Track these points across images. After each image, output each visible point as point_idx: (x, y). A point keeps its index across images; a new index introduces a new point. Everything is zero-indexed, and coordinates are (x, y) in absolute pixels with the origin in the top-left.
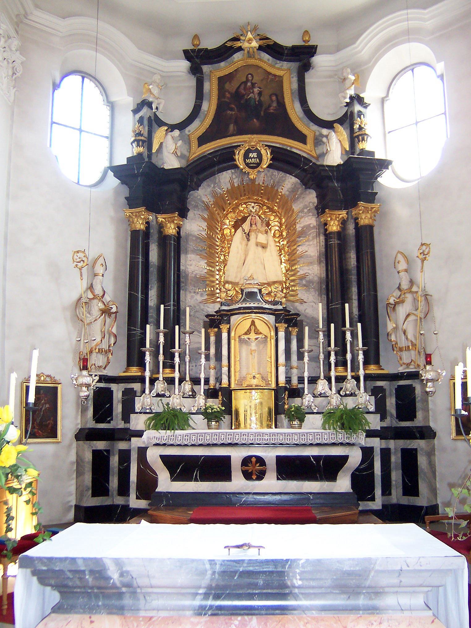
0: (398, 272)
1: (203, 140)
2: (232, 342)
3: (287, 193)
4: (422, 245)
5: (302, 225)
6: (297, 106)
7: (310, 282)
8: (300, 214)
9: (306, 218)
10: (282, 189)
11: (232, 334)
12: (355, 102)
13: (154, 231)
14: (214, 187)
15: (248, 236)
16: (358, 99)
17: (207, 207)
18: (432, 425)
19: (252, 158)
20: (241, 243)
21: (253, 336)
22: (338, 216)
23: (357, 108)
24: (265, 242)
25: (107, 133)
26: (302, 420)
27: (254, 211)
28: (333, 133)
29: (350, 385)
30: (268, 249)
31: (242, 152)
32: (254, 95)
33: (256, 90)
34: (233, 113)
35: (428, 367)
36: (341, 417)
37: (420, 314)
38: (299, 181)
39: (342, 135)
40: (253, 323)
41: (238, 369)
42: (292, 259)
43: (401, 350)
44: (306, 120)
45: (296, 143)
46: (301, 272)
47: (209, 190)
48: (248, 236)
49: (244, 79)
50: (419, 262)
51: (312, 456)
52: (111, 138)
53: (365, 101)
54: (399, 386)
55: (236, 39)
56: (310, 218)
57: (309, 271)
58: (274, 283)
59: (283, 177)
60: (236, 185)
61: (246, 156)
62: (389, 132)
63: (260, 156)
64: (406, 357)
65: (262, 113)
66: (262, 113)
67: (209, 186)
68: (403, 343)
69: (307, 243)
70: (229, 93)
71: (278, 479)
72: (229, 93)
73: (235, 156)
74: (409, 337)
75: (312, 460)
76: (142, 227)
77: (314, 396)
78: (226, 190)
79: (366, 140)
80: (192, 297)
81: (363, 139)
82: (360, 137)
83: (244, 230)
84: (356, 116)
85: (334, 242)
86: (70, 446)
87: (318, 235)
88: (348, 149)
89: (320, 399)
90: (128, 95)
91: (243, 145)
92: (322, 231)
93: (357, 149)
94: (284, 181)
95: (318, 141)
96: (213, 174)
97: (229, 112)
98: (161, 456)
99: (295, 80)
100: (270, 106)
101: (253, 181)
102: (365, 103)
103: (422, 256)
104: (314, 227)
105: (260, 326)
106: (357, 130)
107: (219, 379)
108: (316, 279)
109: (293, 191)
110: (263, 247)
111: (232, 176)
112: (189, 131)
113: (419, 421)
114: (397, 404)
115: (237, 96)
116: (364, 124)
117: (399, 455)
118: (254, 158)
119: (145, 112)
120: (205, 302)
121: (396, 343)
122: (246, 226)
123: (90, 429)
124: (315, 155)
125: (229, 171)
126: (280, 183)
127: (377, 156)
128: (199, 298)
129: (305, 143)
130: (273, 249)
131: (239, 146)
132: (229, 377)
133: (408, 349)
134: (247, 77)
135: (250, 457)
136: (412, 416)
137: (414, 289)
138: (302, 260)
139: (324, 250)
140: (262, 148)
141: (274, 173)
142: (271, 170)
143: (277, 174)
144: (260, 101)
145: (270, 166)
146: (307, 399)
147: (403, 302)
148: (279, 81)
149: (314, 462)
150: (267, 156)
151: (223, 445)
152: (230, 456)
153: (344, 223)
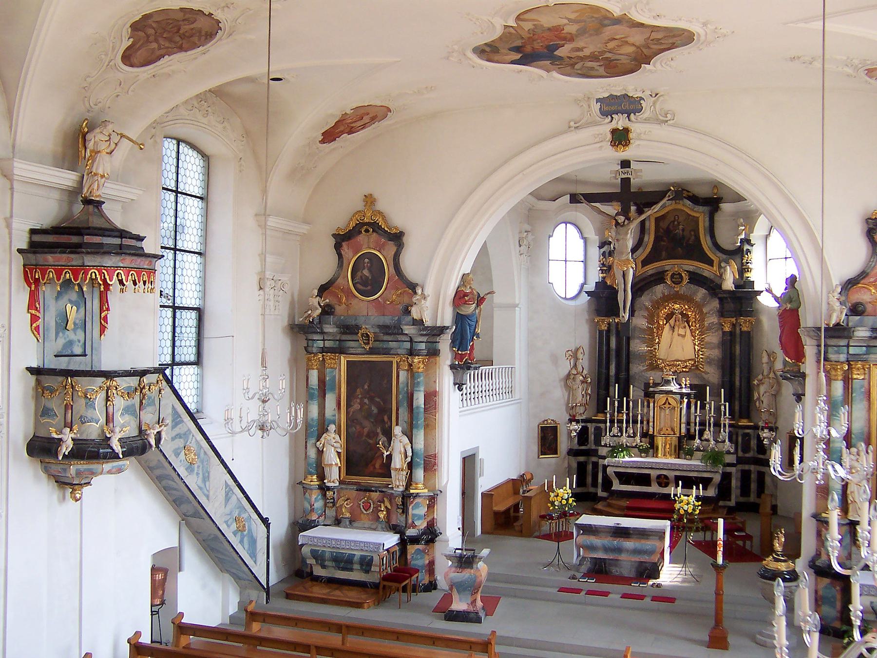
1: (645, 263)
2: (656, 409)
5: (709, 322)
6: (708, 238)
7: (713, 360)
11: (656, 405)
12: (745, 243)
13: (613, 329)
14: (652, 295)
16: (748, 241)
17: (647, 308)
19: (676, 278)
23: (746, 247)
25: (582, 258)
26: (692, 456)
32: (679, 231)
33: (681, 227)
41: (658, 424)
44: (714, 249)
46: (707, 354)
47: (649, 296)
48: (673, 328)
49: (673, 219)
52: (585, 262)
58: (690, 360)
60: (666, 294)
63: (681, 277)
67: (648, 294)
70: (663, 229)
72: (663, 229)
76: (606, 328)
77: (701, 440)
84: (745, 253)
86: (565, 458)
90: (596, 235)
98: (614, 472)
99: (707, 219)
100: (689, 239)
101: (678, 291)
105: (671, 400)
107: (648, 430)
108: (716, 358)
109: (704, 299)
115: (668, 231)
117: (756, 473)
119: (605, 248)
120: (647, 370)
122: (672, 321)
123: (576, 450)
125: (662, 285)
126: (695, 293)
128: (641, 368)
129: (713, 266)
130: (688, 336)
132: (654, 428)
134: (675, 218)
144: (683, 235)
146: (697, 441)
147: (763, 383)
148: (696, 221)
152: (650, 474)
153: (734, 325)
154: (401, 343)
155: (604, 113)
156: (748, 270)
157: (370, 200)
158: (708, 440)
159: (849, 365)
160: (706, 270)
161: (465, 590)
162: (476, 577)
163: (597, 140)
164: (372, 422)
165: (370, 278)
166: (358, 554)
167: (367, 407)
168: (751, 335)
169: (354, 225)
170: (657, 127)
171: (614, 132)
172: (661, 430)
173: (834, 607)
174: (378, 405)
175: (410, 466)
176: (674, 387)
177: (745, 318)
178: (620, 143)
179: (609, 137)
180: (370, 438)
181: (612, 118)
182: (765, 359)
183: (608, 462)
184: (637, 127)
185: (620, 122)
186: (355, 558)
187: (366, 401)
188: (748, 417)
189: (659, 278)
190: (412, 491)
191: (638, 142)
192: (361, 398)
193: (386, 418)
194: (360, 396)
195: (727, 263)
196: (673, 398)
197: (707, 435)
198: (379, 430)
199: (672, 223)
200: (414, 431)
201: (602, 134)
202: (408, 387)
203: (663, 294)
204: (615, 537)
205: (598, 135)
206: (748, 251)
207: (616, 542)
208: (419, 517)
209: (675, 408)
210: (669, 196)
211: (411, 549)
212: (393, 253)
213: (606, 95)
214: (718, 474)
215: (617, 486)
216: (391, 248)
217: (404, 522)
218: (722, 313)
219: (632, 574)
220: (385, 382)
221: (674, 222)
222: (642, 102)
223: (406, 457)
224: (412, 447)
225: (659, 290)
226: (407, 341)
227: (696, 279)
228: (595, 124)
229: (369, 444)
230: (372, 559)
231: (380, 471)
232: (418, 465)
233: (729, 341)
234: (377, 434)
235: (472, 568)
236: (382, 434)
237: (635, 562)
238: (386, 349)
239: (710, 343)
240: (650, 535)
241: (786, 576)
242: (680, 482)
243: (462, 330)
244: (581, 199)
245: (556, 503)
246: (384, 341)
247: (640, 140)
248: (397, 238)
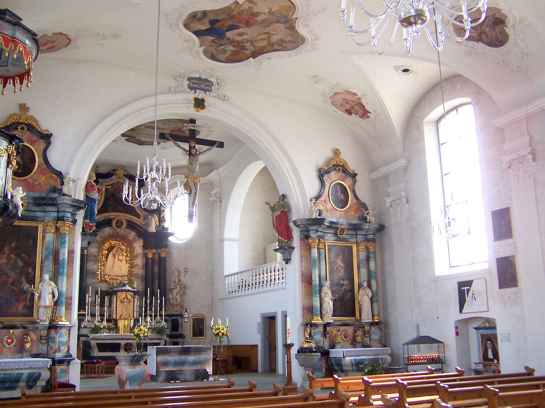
0: (175, 276)
4: (185, 268)
11: (118, 300)
15: (114, 255)
18: (184, 333)
19: (118, 224)
21: (125, 300)
24: (121, 259)
29: (158, 318)
30: (123, 262)
31: (115, 221)
35: (186, 313)
36: (159, 330)
37: (182, 292)
40: (126, 296)
42: (132, 266)
43: (174, 305)
49: (116, 188)
50: (184, 275)
54: (173, 319)
55: (114, 170)
61: (117, 223)
63: (122, 223)
64: (176, 308)
68: (175, 303)
74: (178, 301)
80: (91, 280)
84: (162, 211)
85: (150, 262)
87: (143, 257)
92: (145, 256)
95: (145, 218)
97: (109, 202)
103: (185, 273)
105: (129, 297)
106: (162, 218)
108: (141, 275)
110: (121, 261)
113: (180, 332)
114: (172, 325)
121: (172, 303)
122: (114, 251)
129: (139, 218)
130: (124, 261)
132: (116, 315)
133: (177, 305)
135: (128, 343)
136: (177, 330)
137: (181, 283)
138: (136, 267)
139: (145, 264)
147: (176, 288)
151: (119, 339)
153: (154, 254)
154: (48, 213)
155: (190, 87)
156: (164, 221)
157: (23, 108)
159: (319, 241)
160: (139, 221)
161: (135, 382)
162: (145, 371)
163: (186, 102)
164: (18, 273)
165: (21, 163)
166: (26, 372)
167: (13, 261)
169: (11, 123)
170: (221, 101)
171: (196, 99)
172: (122, 315)
173: (322, 372)
174: (23, 260)
175: (56, 304)
176: (128, 288)
178: (199, 107)
179: (193, 102)
180: (15, 286)
181: (195, 91)
183: (92, 337)
184: (209, 99)
185: (200, 95)
186: (24, 376)
187: (13, 256)
189: (108, 223)
190: (60, 323)
191: (209, 108)
192: (8, 254)
193: (30, 270)
194: (7, 252)
195: (152, 216)
196: (129, 294)
198: (23, 279)
199: (115, 191)
200: (60, 278)
201: (189, 99)
202: (53, 245)
203: (109, 233)
204: (181, 354)
205: (186, 99)
207: (182, 358)
208: (63, 344)
209: (130, 301)
210: (217, 144)
211: (59, 368)
212: (43, 148)
213: (198, 76)
215: (96, 353)
216: (42, 145)
217: (46, 351)
218: (145, 247)
219: (193, 378)
220: (31, 242)
221: (117, 189)
222: (212, 86)
223: (54, 297)
224: (58, 289)
225: (107, 231)
226: (55, 212)
227: (131, 225)
228: (185, 92)
229: (13, 290)
230: (40, 375)
231: (24, 312)
232: (61, 304)
233: (148, 265)
234: (22, 282)
235: (140, 365)
236: (26, 282)
237: (193, 370)
238: (34, 217)
240: (201, 351)
241: (314, 350)
242: (213, 318)
243: (91, 209)
244: (168, 137)
245: (141, 335)
246: (31, 211)
247: (210, 107)
248: (47, 138)
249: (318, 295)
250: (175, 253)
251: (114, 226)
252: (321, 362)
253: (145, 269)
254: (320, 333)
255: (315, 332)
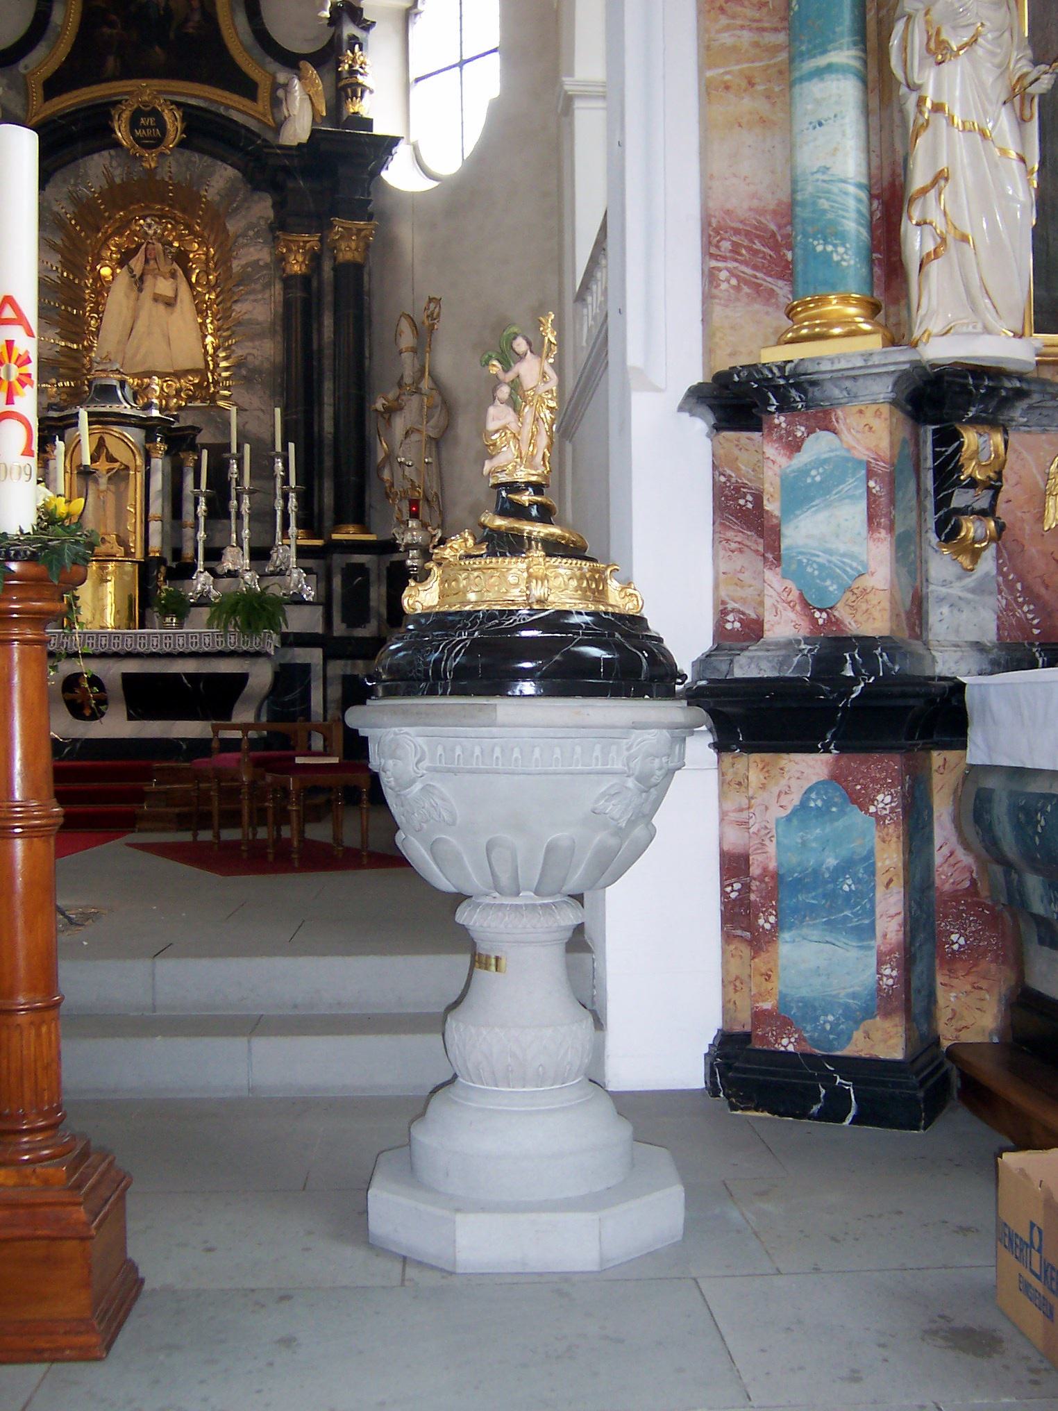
3: (217, 198)
5: (243, 262)
6: (242, 20)
7: (255, 371)
8: (241, 240)
9: (252, 249)
10: (206, 191)
12: (346, 18)
14: (76, 185)
19: (145, 127)
20: (128, 297)
22: (302, 244)
23: (349, 29)
24: (170, 294)
27: (151, 232)
28: (296, 81)
34: (115, 31)
38: (239, 175)
39: (313, 84)
44: (258, 51)
45: (236, 97)
48: (139, 282)
51: (185, 674)
53: (366, 16)
54: (392, 563)
56: (259, 248)
57: (255, 352)
59: (208, 166)
60: (118, 181)
61: (134, 124)
62: (417, 80)
63: (161, 124)
65: (172, 35)
66: (172, 35)
67: (65, 181)
69: (252, 297)
71: (130, 718)
73: (112, 121)
75: (186, 681)
78: (98, 190)
79: (359, 95)
81: (355, 95)
82: (349, 91)
83: (131, 271)
84: (345, 46)
88: (324, 114)
89: (226, 581)
91: (127, 100)
93: (344, 112)
94: (211, 175)
96: (75, 159)
97: (106, 31)
100: (187, 20)
101: (152, 172)
102: (365, 19)
104: (267, 266)
106: (345, 75)
108: (266, 365)
109: (229, 194)
111: (111, 163)
112: (26, 67)
116: (359, 62)
118: (150, 127)
122: (137, 263)
124: (271, 122)
125: (105, 153)
127: (377, 130)
129: (253, 97)
131: (120, 102)
139: (280, 310)
140: (164, 106)
141: (193, 159)
142: (187, 153)
143: (198, 161)
145: (182, 144)
146: (202, 581)
149: (189, 685)
150: (174, 123)
158: (232, 574)
168: (366, 288)
176: (126, 408)
177: (349, 224)
182: (407, 339)
188: (361, 521)
197: (236, 559)
206: (354, 40)
209: (127, 468)
214: (261, 660)
218: (281, 225)
239: (250, 322)
249: (845, 55)
250: (409, 237)
251: (121, 134)
252: (856, 817)
253: (279, 338)
254: (855, 485)
255: (804, 472)
